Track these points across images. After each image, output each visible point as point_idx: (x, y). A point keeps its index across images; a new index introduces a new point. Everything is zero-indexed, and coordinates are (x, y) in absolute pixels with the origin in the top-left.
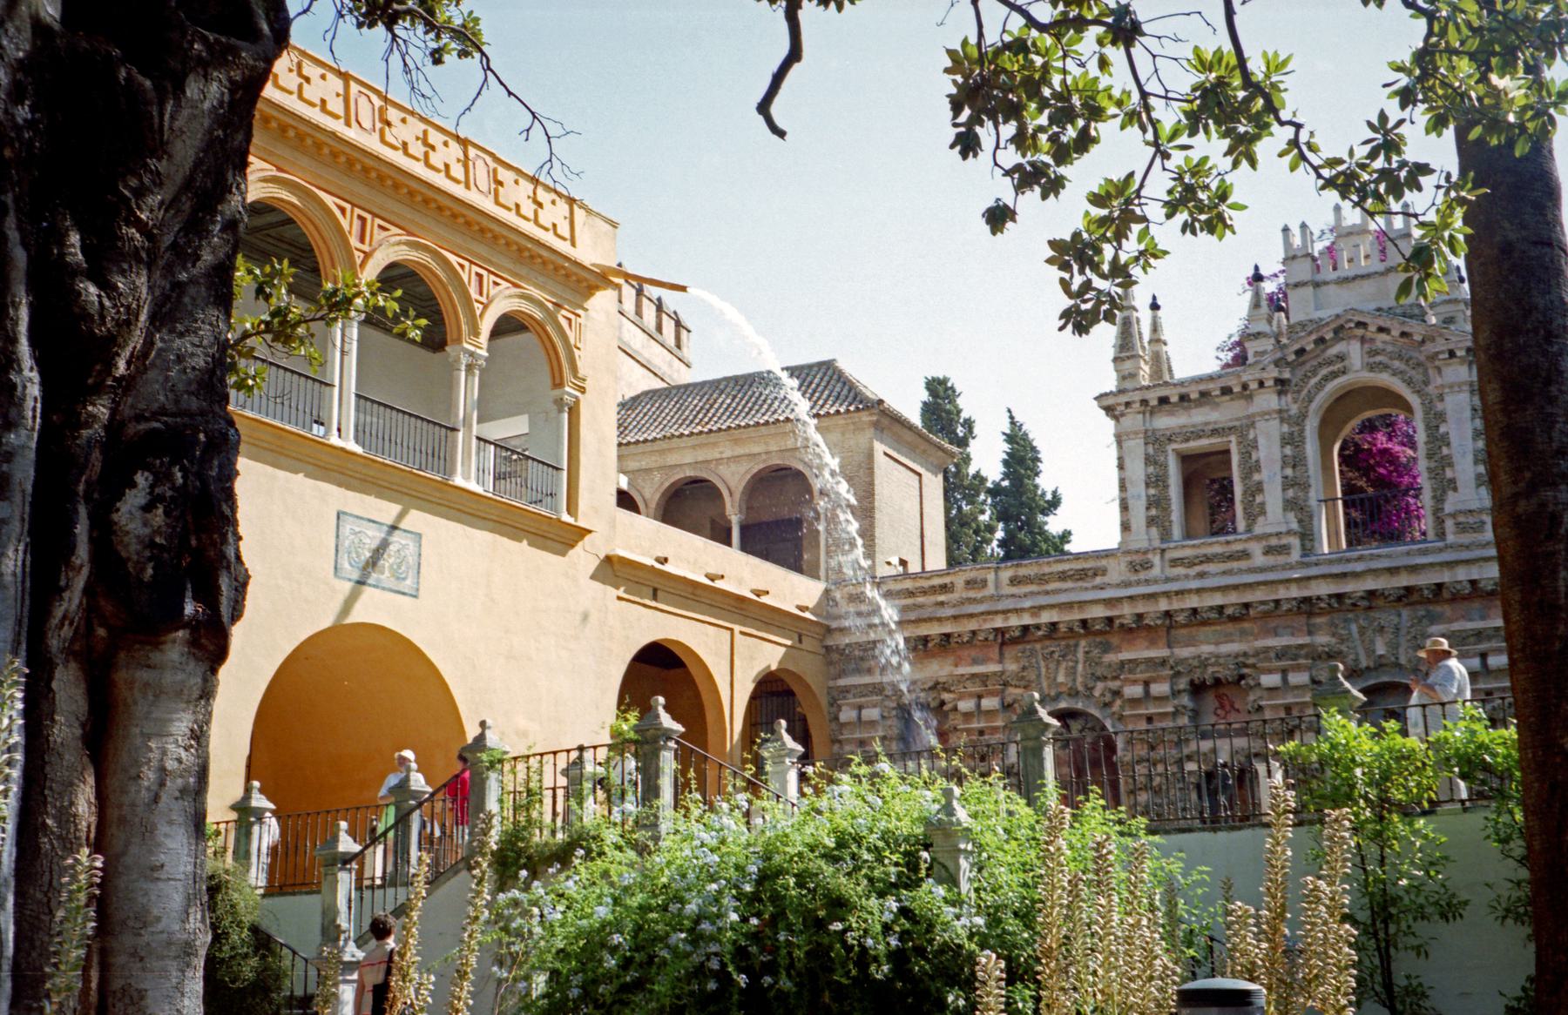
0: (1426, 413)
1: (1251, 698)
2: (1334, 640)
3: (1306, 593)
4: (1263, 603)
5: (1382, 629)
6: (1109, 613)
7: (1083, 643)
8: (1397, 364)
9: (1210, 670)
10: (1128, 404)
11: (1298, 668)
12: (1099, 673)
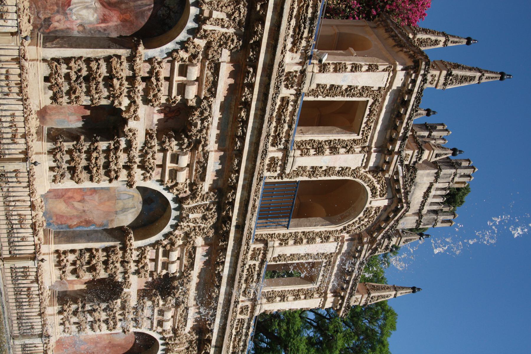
0: (330, 232)
4: (239, 164)
5: (204, 218)
8: (366, 220)
9: (199, 122)
10: (414, 82)
12: (213, 44)
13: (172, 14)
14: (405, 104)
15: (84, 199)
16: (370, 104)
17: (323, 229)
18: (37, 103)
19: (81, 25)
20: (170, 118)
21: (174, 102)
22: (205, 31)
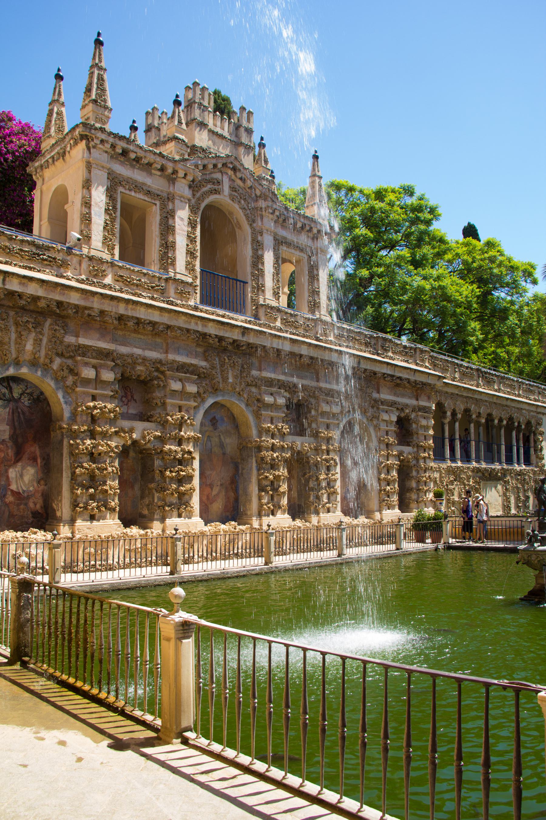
1: (158, 394)
2: (208, 366)
3: (206, 330)
5: (233, 366)
6: (82, 303)
7: (49, 321)
9: (139, 368)
10: (102, 141)
11: (188, 380)
13: (28, 391)
14: (125, 153)
15: (210, 485)
16: (123, 190)
17: (249, 246)
18: (115, 527)
19: (39, 482)
20: (132, 397)
21: (117, 392)
22: (46, 357)
